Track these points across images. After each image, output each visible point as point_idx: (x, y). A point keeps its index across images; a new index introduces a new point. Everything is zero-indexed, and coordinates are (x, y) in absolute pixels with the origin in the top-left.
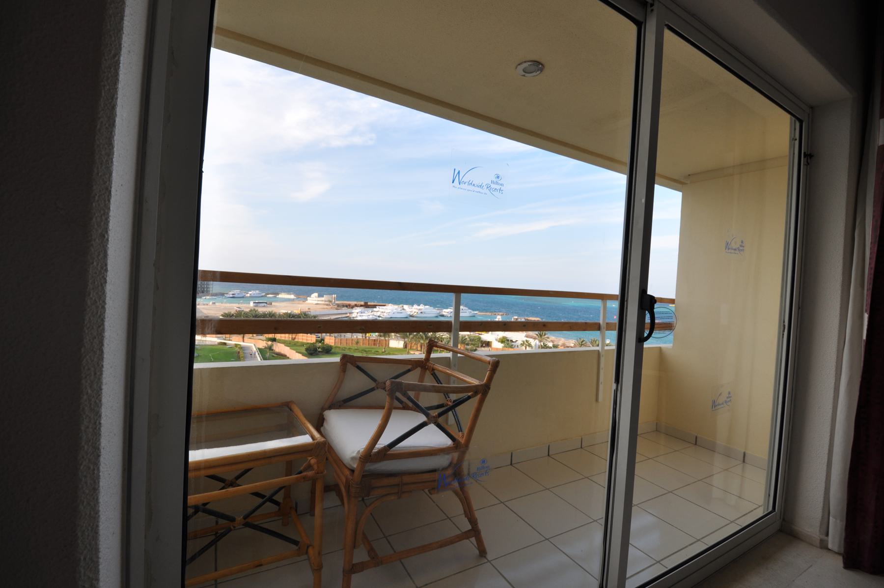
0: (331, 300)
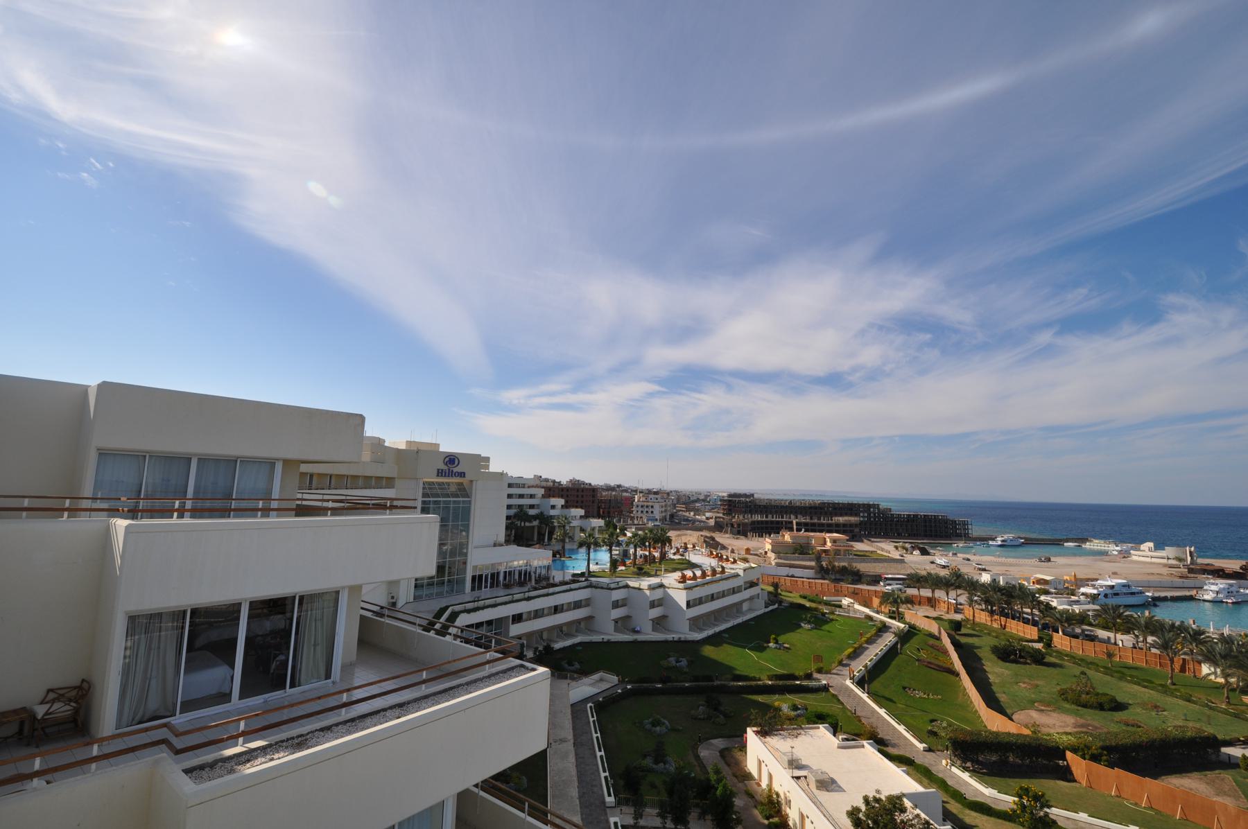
0: (1183, 556)
